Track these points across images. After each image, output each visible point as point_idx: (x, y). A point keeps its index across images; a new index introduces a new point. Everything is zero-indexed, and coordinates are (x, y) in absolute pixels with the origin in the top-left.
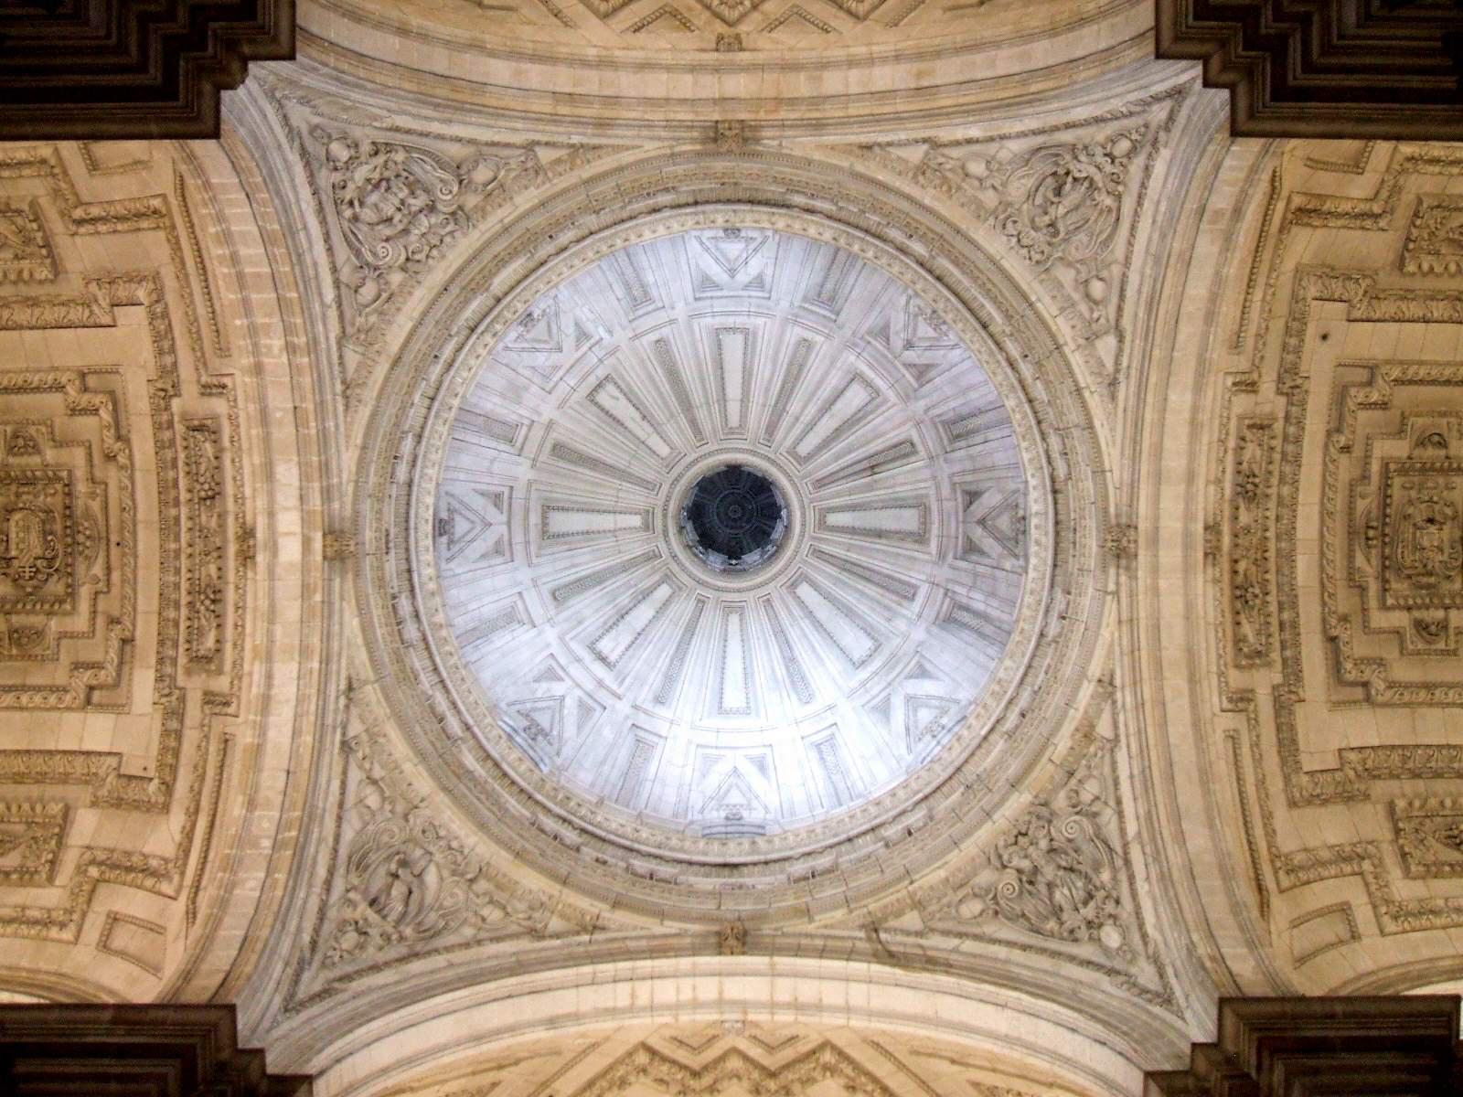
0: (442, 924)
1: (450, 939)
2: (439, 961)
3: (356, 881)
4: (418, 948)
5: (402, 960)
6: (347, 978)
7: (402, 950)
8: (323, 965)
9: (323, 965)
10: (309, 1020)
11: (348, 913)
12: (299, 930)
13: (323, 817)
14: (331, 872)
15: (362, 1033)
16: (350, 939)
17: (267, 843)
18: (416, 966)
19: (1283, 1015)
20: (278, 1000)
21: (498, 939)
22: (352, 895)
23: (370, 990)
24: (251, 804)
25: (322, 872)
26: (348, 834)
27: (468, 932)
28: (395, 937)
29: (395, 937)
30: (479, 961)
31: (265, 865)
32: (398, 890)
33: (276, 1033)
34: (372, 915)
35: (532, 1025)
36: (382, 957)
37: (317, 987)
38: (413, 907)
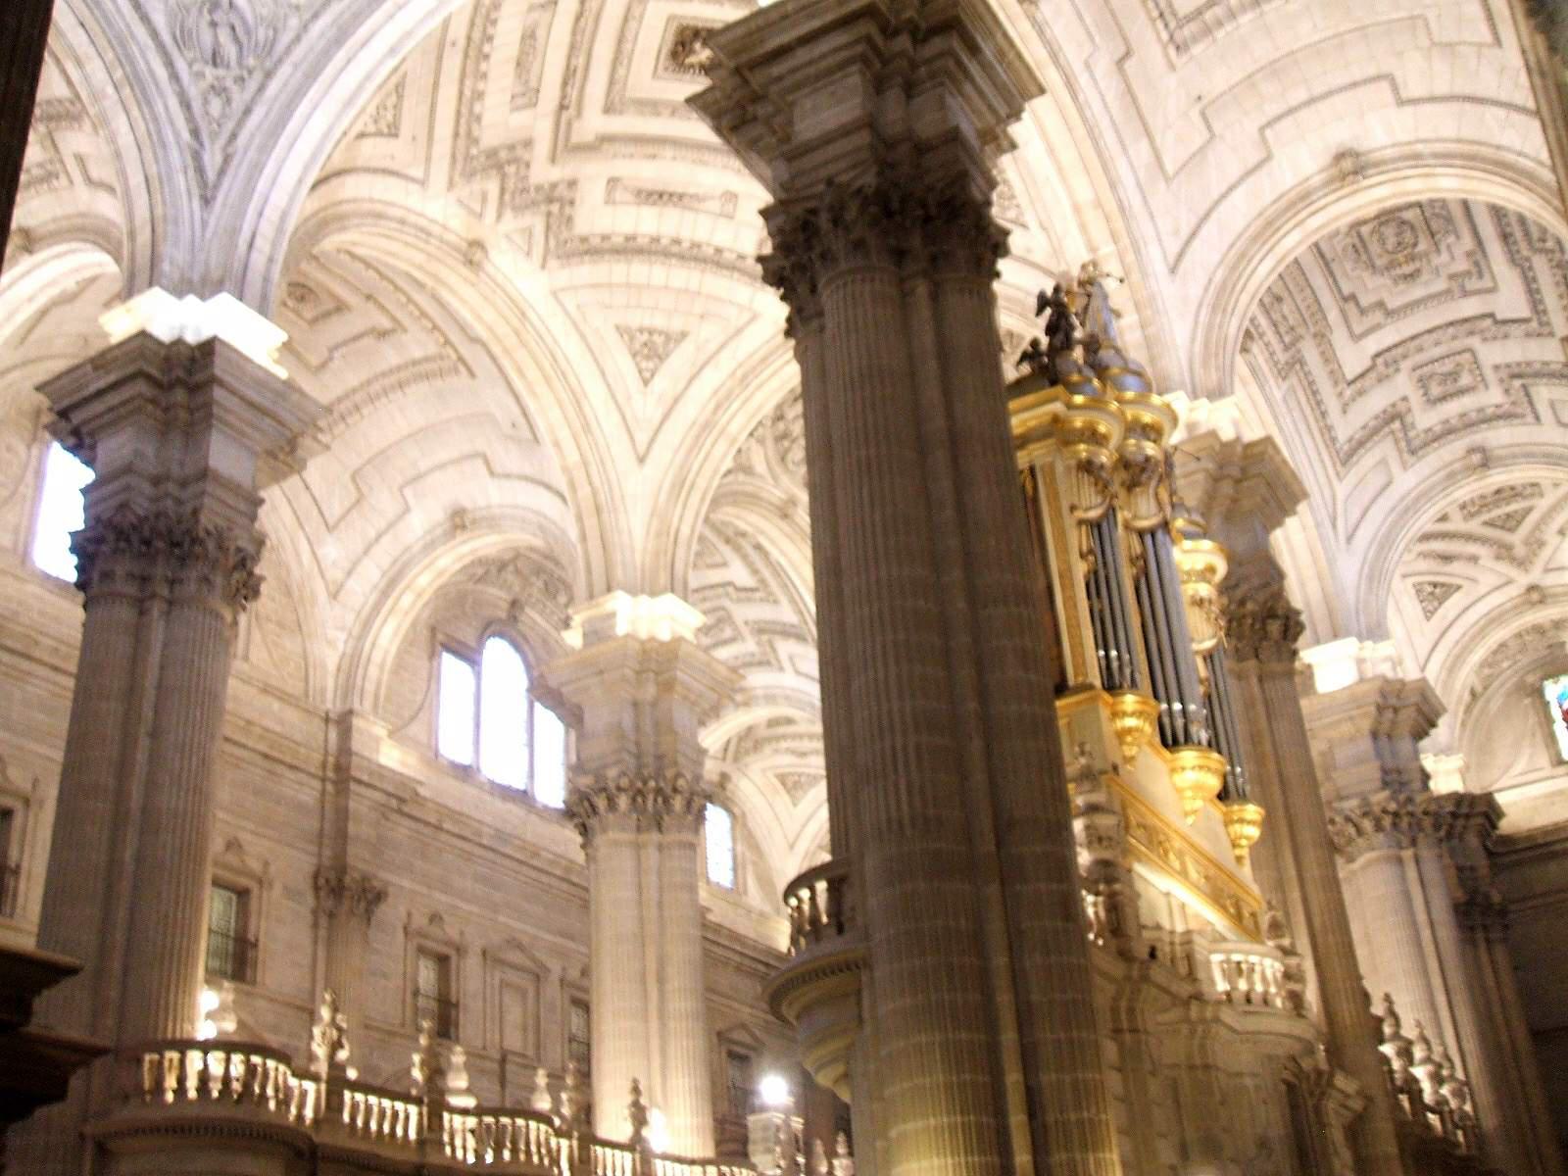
0: (271, 33)
1: (285, 39)
2: (285, 70)
3: (190, 55)
4: (268, 64)
5: (261, 89)
6: (234, 136)
7: (258, 76)
8: (213, 142)
9: (213, 142)
10: (224, 205)
11: (204, 85)
12: (177, 135)
13: (132, 34)
14: (169, 64)
15: (262, 186)
16: (216, 106)
17: (110, 90)
18: (273, 87)
19: (750, 34)
20: (196, 203)
21: (316, 16)
22: (196, 67)
23: (252, 136)
24: (79, 63)
25: (162, 73)
26: (160, 20)
27: (294, 22)
28: (245, 74)
29: (245, 74)
30: (312, 49)
31: (119, 107)
32: (224, 36)
33: (208, 235)
34: (221, 72)
35: (380, 63)
36: (247, 95)
37: (219, 159)
38: (243, 38)
